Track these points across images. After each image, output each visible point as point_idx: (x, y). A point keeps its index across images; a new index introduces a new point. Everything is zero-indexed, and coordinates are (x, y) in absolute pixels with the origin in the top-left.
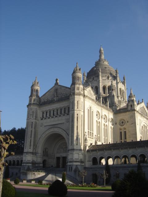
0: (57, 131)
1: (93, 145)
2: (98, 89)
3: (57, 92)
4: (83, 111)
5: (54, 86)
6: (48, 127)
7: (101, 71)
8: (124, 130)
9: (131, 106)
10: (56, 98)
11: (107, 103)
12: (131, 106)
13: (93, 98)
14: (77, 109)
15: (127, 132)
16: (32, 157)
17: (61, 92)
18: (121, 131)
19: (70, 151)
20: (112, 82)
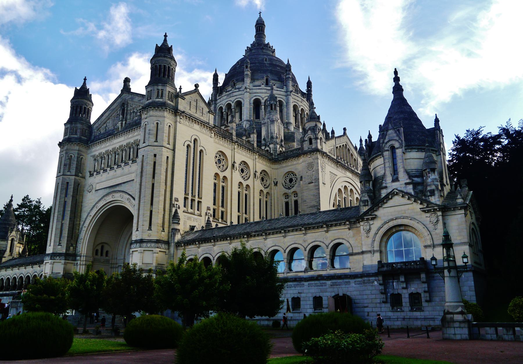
1: (195, 229)
3: (123, 110)
4: (171, 147)
5: (120, 96)
7: (249, 66)
8: (296, 198)
9: (310, 140)
10: (122, 124)
11: (252, 136)
12: (310, 140)
13: (204, 119)
14: (156, 144)
15: (299, 202)
16: (62, 266)
17: (133, 109)
18: (287, 200)
19: (132, 246)
20: (272, 89)
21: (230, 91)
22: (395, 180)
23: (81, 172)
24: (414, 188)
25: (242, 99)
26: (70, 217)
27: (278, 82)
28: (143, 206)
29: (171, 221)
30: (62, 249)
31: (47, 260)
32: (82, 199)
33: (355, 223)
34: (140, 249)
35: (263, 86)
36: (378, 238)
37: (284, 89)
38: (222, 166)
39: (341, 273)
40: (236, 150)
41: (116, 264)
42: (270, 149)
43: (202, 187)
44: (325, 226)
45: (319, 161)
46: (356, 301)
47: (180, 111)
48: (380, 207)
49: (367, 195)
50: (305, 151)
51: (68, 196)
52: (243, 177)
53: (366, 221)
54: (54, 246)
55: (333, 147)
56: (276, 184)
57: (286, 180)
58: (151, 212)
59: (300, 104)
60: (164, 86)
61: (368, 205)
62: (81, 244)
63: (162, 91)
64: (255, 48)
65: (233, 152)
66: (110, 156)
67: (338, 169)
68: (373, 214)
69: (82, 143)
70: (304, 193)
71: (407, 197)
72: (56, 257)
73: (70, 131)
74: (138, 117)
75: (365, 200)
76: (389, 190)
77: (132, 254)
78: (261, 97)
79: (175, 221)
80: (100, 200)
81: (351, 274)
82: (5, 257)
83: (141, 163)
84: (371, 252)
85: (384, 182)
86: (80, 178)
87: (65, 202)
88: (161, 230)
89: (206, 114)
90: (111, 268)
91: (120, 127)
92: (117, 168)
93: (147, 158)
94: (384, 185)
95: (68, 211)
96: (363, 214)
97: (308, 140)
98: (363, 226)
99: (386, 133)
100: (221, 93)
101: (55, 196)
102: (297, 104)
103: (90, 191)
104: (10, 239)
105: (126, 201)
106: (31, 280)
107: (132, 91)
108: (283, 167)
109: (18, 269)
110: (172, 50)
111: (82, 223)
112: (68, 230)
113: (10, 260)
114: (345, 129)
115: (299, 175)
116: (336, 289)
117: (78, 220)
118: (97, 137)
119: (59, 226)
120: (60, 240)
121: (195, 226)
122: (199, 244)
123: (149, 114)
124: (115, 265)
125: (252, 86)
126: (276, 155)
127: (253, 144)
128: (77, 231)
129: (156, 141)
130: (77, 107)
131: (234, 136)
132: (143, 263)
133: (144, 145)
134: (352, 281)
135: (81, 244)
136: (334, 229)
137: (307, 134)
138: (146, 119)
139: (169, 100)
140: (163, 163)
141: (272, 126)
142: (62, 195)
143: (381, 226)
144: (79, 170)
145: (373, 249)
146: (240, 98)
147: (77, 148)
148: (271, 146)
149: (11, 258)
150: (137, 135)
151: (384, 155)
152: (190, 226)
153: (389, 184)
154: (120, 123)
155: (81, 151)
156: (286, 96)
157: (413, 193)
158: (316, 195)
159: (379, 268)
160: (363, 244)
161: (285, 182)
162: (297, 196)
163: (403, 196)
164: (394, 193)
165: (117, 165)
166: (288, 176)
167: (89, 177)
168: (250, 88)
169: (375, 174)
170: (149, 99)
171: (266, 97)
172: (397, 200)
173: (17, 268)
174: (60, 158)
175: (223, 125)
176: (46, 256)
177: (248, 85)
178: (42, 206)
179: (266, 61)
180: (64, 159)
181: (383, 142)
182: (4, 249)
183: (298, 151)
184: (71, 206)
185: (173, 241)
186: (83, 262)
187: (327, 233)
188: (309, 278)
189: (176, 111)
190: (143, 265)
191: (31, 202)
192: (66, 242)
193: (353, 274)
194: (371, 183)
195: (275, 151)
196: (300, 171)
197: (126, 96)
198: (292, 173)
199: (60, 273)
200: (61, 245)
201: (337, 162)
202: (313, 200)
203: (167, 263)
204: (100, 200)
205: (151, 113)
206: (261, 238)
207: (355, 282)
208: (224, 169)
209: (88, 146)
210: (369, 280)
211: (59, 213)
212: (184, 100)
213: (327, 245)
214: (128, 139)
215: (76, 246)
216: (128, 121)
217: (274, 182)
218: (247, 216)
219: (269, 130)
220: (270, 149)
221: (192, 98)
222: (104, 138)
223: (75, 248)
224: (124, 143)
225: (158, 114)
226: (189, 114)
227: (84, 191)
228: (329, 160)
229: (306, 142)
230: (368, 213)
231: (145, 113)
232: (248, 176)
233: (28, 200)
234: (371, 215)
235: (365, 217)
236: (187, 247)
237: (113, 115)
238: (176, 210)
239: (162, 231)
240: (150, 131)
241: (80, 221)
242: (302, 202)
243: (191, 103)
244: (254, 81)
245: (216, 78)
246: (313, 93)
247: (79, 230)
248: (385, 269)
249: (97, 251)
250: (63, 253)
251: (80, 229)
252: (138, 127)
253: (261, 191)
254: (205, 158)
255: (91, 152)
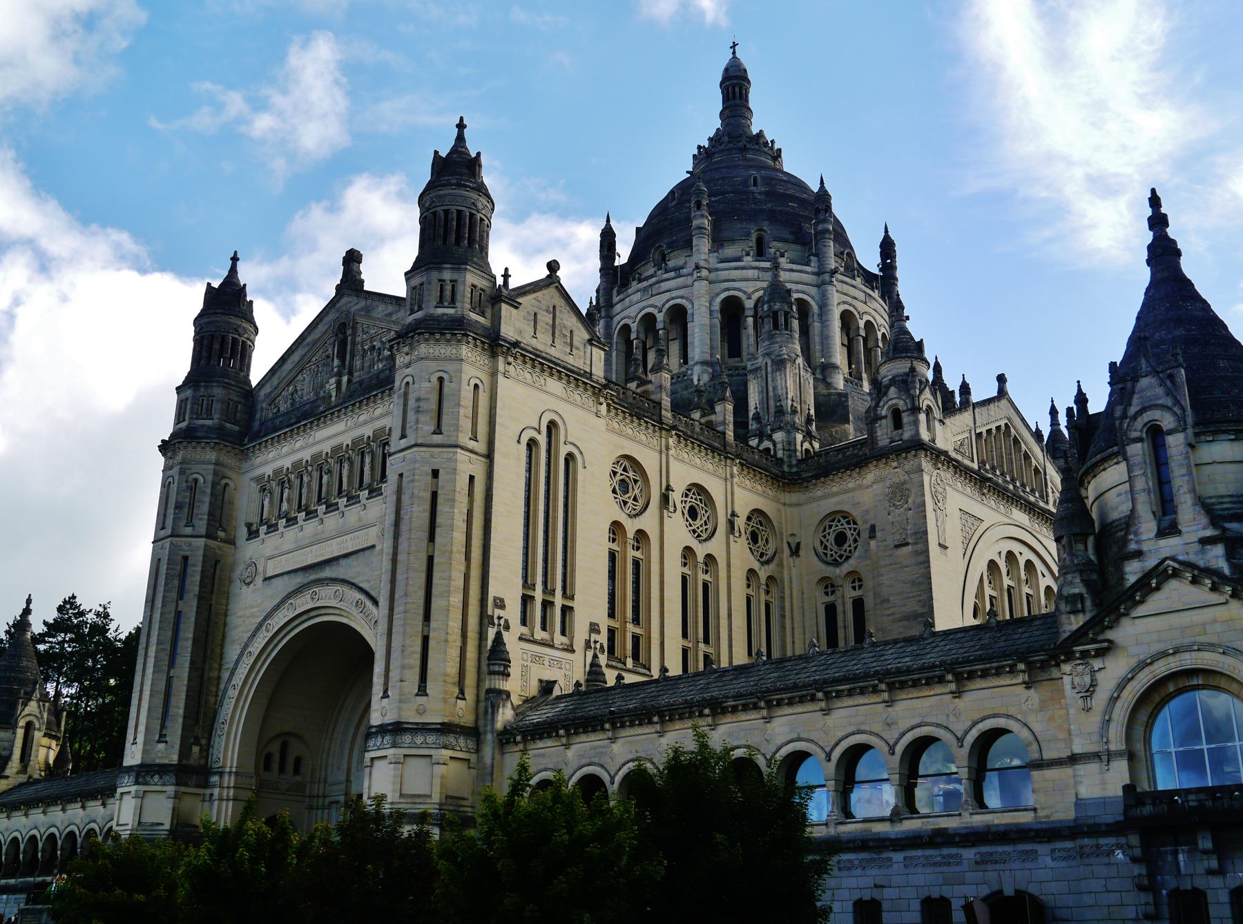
0: (333, 603)
1: (556, 692)
2: (689, 325)
3: (343, 344)
4: (481, 446)
5: (332, 304)
6: (282, 587)
7: (705, 203)
8: (858, 593)
10: (339, 383)
11: (718, 408)
14: (437, 439)
15: (869, 603)
17: (372, 339)
18: (830, 599)
19: (371, 743)
20: (776, 267)
21: (652, 276)
22: (1168, 529)
23: (224, 526)
24: (1229, 556)
25: (687, 299)
26: (191, 657)
27: (794, 246)
28: (402, 622)
29: (484, 668)
30: (169, 754)
31: (127, 786)
32: (227, 605)
33: (1044, 666)
34: (392, 751)
35: (748, 260)
36: (1120, 713)
37: (812, 265)
38: (631, 501)
39: (1005, 825)
40: (672, 452)
41: (324, 797)
42: (775, 445)
43: (573, 566)
44: (950, 677)
45: (926, 478)
46: (1058, 913)
47: (505, 341)
48: (1126, 615)
49: (1078, 580)
50: (882, 448)
51: (186, 596)
52: (694, 531)
53: (1079, 659)
54: (145, 744)
55: (968, 435)
56: (795, 551)
57: (825, 537)
58: (426, 640)
59: (861, 307)
60: (459, 269)
61: (1083, 611)
62: (224, 738)
63: (453, 286)
64: (722, 147)
65: (664, 456)
66: (305, 479)
67: (985, 502)
68: (1101, 637)
69: (226, 441)
70: (882, 575)
71: (1208, 582)
72: (152, 778)
73: (192, 408)
74: (384, 363)
75: (1075, 595)
76: (1151, 563)
77: (371, 766)
78: (745, 292)
79: (496, 668)
80: (277, 607)
81: (1040, 826)
82: (7, 777)
83: (395, 497)
84: (1099, 757)
85: (1132, 537)
86: (222, 544)
87: (178, 614)
88: (455, 695)
89: (582, 348)
90: (311, 808)
91: (334, 394)
92: (325, 513)
93: (413, 481)
94: (1133, 546)
95: (186, 639)
96: (1068, 638)
97: (890, 416)
98: (1070, 677)
99: (1133, 387)
100: (625, 285)
101: (150, 599)
102: (852, 309)
103: (248, 580)
104: (22, 723)
105: (354, 608)
106: (79, 846)
107: (367, 287)
108: (815, 499)
109: (44, 813)
110: (480, 166)
111: (226, 675)
112: (187, 696)
113: (21, 785)
114: (1001, 379)
115: (865, 522)
116: (991, 875)
117: (216, 666)
118: (269, 424)
119: (162, 686)
120: (163, 726)
121: (555, 682)
122: (568, 735)
123: (416, 353)
124: (321, 800)
125: (715, 261)
126: (794, 462)
127: (724, 433)
128: (212, 699)
129: (438, 431)
130: (212, 337)
131: (666, 410)
132: (401, 795)
133: (404, 443)
134: (1043, 849)
135: (224, 738)
136: (978, 686)
137: (885, 398)
138: (407, 367)
139: (473, 309)
140: (457, 495)
141: (779, 378)
142: (169, 594)
143: (1130, 676)
144: (219, 520)
145: (1106, 747)
146: (682, 297)
147: (212, 456)
148: (779, 436)
149: (23, 778)
150: (382, 416)
151: (1129, 454)
152: (541, 681)
153: (1148, 542)
154: (333, 380)
155: (223, 465)
156: (818, 286)
157: (1227, 571)
158: (920, 583)
159: (1127, 807)
160: (1073, 733)
161: (822, 542)
162: (860, 587)
163: (1194, 581)
164: (1165, 570)
165: (325, 503)
166: (830, 527)
167: (247, 540)
168: (711, 266)
169: (1103, 515)
170: (416, 308)
171: (757, 291)
172: (1177, 592)
173: (41, 810)
174: (163, 486)
175: (632, 380)
176: (121, 772)
177: (703, 257)
178: (112, 626)
179: (755, 185)
180: (174, 487)
181: (1124, 416)
182: (5, 753)
183: (860, 450)
184: (196, 625)
185: (489, 728)
186: (228, 793)
187: (957, 700)
188: (907, 838)
189: (494, 344)
190: (402, 801)
191: (82, 614)
192: (179, 732)
193: (1044, 826)
194: (1091, 540)
195: (789, 450)
196: (867, 511)
197: (352, 304)
198: (844, 518)
199: (163, 824)
200: (166, 742)
201: (980, 481)
202: (909, 598)
203: (473, 793)
204: (277, 607)
205: (423, 349)
206: (754, 715)
207: (1053, 851)
208: (638, 508)
209: (242, 451)
210: (1098, 846)
211: (161, 647)
212: (516, 308)
213: (959, 736)
214: (357, 426)
215: (209, 745)
216: (356, 374)
217: (789, 543)
218: (711, 650)
219: (771, 389)
220: (775, 445)
221: (538, 301)
222: (288, 426)
223: (206, 750)
224: (347, 440)
225: (443, 351)
226: (531, 349)
227: (231, 581)
228: (956, 473)
229: (884, 421)
230: (1086, 634)
231: (406, 349)
232: (710, 527)
233: (74, 609)
234: (1094, 641)
235: (1075, 649)
236: (531, 746)
237: (314, 359)
238: (499, 636)
239: (457, 698)
240: (421, 404)
241: (220, 670)
242: (876, 605)
243: (539, 317)
244: (722, 246)
245: (608, 240)
246: (898, 274)
247: (217, 695)
248: (1148, 809)
249: (268, 758)
250: (171, 765)
251: (220, 694)
252: (384, 392)
253: (751, 572)
254: (582, 477)
255: (254, 468)
